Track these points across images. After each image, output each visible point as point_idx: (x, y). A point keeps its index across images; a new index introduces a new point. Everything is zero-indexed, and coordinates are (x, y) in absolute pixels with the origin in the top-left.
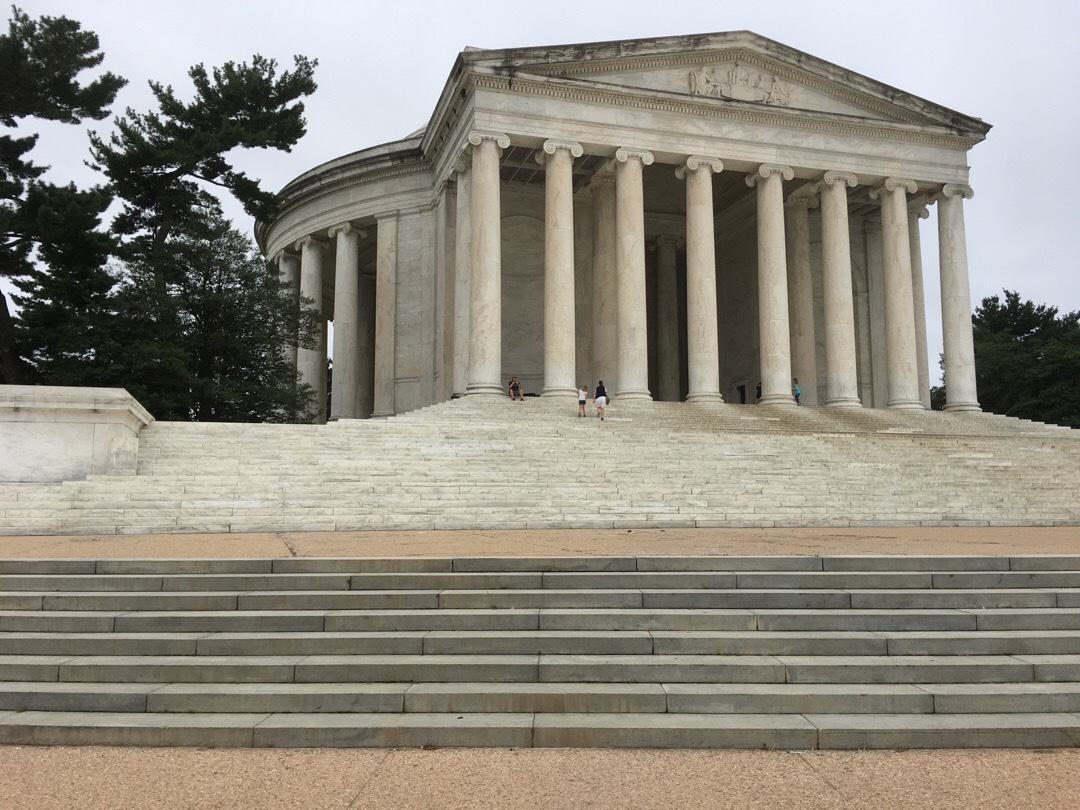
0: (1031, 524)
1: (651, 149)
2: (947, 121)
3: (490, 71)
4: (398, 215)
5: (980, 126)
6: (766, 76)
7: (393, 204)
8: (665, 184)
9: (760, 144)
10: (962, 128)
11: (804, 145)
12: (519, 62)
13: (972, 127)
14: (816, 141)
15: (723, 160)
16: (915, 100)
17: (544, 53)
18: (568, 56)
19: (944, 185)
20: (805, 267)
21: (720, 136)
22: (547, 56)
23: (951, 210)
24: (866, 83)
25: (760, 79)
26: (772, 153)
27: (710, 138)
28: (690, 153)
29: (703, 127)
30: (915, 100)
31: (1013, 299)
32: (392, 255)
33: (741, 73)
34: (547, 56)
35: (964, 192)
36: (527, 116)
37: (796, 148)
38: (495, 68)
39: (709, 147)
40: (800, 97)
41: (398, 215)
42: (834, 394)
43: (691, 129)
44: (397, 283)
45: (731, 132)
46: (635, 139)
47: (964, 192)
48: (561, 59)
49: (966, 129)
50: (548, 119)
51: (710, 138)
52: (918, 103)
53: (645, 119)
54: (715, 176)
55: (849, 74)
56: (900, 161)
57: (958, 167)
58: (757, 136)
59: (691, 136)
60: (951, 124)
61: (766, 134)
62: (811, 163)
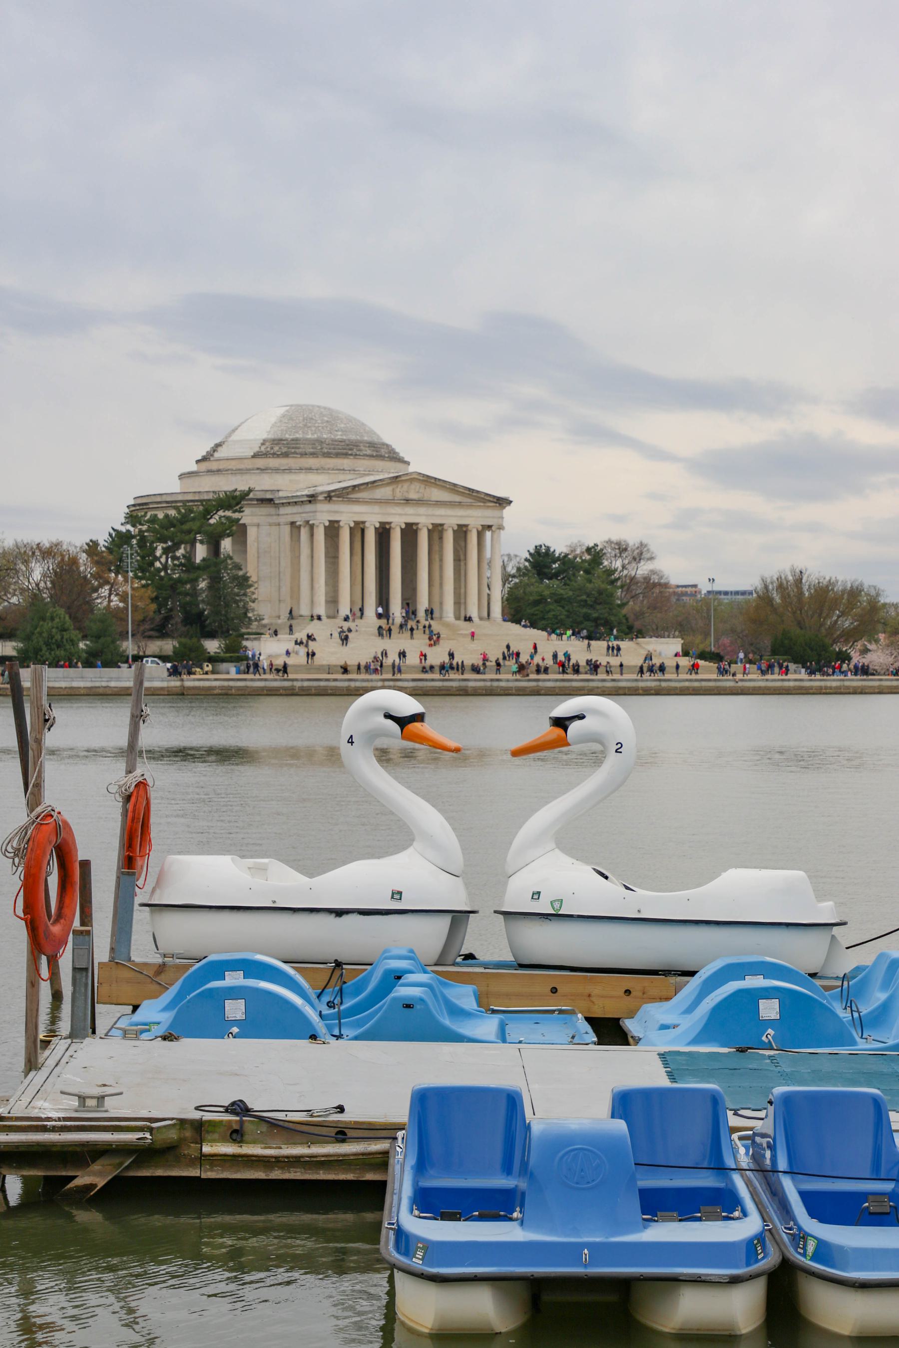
0: (859, 690)
4: (258, 525)
6: (423, 486)
7: (256, 520)
8: (383, 533)
9: (420, 515)
12: (333, 494)
14: (442, 511)
18: (350, 489)
20: (436, 548)
23: (495, 536)
26: (424, 518)
27: (400, 515)
29: (398, 510)
31: (548, 548)
32: (256, 544)
33: (413, 487)
35: (501, 528)
37: (433, 515)
39: (398, 518)
40: (437, 494)
41: (258, 525)
42: (444, 615)
44: (258, 557)
46: (372, 517)
47: (501, 528)
49: (502, 502)
50: (342, 512)
51: (400, 515)
53: (376, 509)
54: (402, 529)
55: (455, 485)
56: (474, 517)
61: (422, 510)
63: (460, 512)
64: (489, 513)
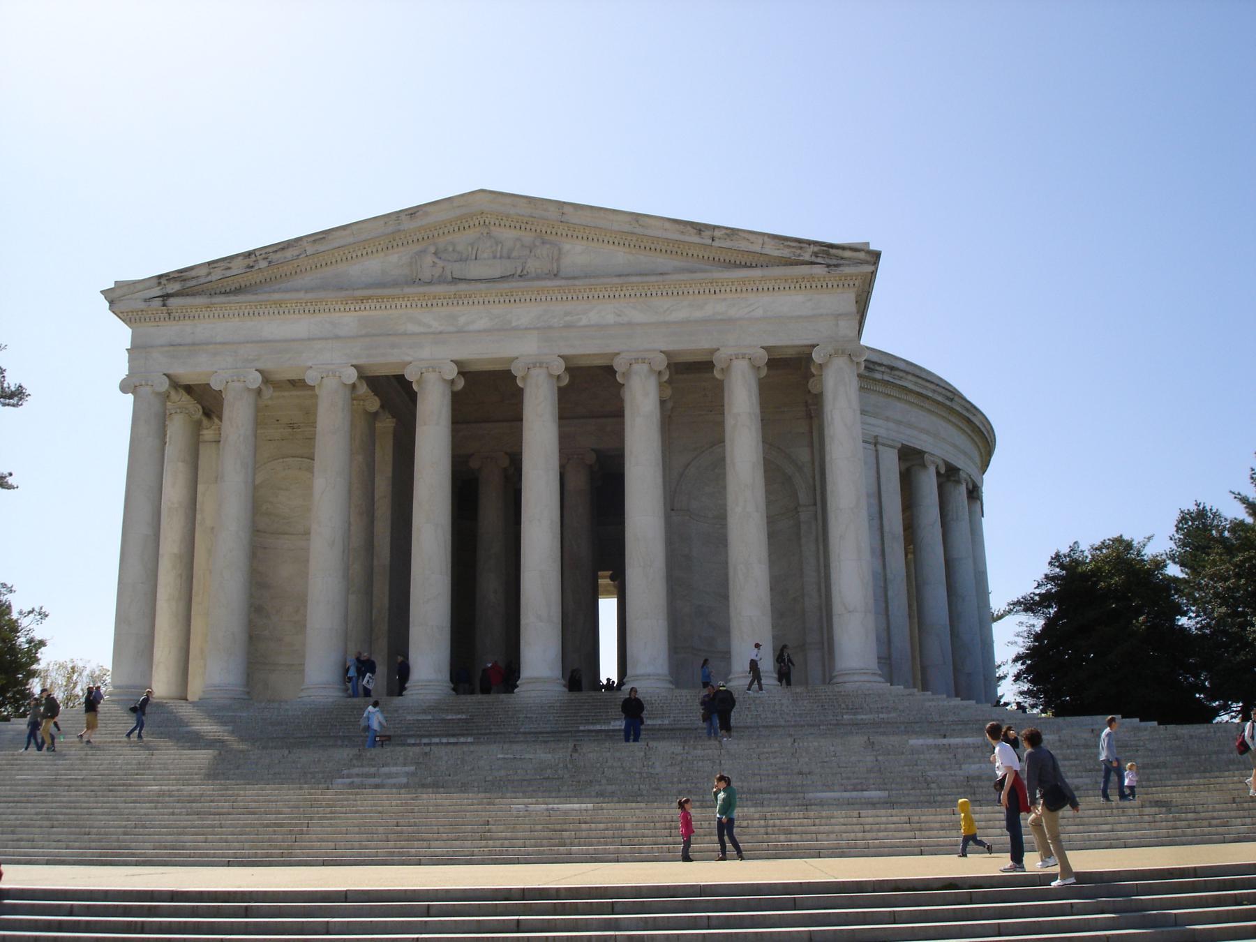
1: (354, 362)
2: (807, 257)
3: (142, 305)
5: (862, 255)
10: (834, 262)
11: (582, 323)
13: (850, 259)
15: (457, 363)
16: (746, 235)
17: (204, 272)
19: (814, 346)
21: (452, 329)
22: (209, 274)
24: (667, 225)
28: (409, 359)
30: (746, 235)
34: (209, 274)
36: (195, 346)
38: (145, 301)
43: (411, 328)
48: (228, 273)
52: (752, 238)
57: (838, 316)
59: (414, 334)
62: (588, 348)
63: (681, 310)
64: (791, 302)
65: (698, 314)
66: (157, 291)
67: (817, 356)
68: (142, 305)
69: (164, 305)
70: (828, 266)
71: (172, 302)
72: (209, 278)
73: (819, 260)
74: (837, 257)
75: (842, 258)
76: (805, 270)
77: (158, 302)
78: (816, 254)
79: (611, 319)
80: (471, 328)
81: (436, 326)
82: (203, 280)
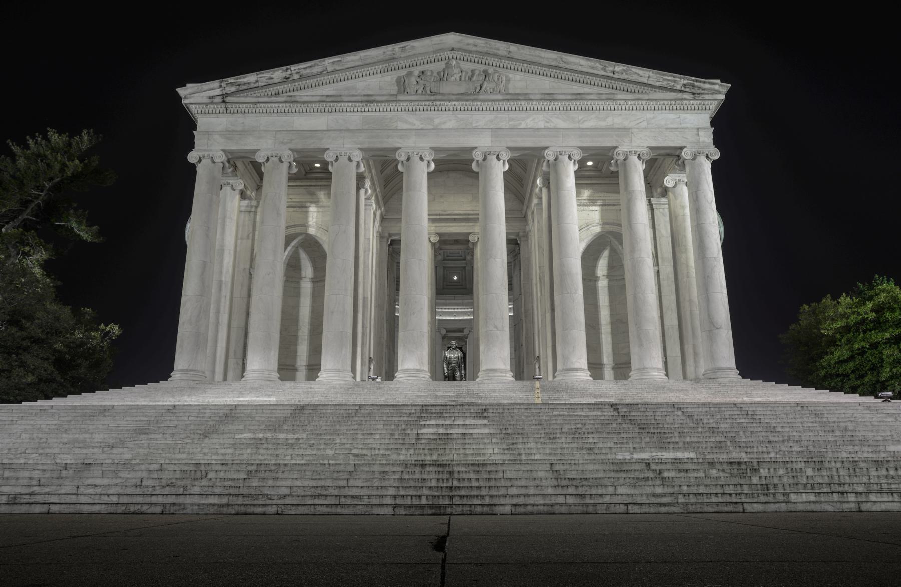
1: (359, 146)
2: (678, 87)
3: (207, 100)
10: (697, 91)
13: (708, 89)
19: (682, 148)
25: (473, 71)
29: (415, 121)
36: (244, 133)
38: (210, 97)
45: (445, 123)
58: (471, 123)
60: (683, 89)
61: (481, 119)
63: (591, 121)
65: (603, 124)
66: (218, 92)
67: (686, 154)
68: (207, 100)
69: (224, 101)
70: (694, 94)
71: (228, 99)
72: (257, 84)
73: (687, 90)
74: (699, 87)
75: (703, 89)
76: (679, 95)
77: (219, 99)
78: (685, 85)
79: (541, 125)
80: (443, 126)
81: (418, 124)
82: (252, 85)
